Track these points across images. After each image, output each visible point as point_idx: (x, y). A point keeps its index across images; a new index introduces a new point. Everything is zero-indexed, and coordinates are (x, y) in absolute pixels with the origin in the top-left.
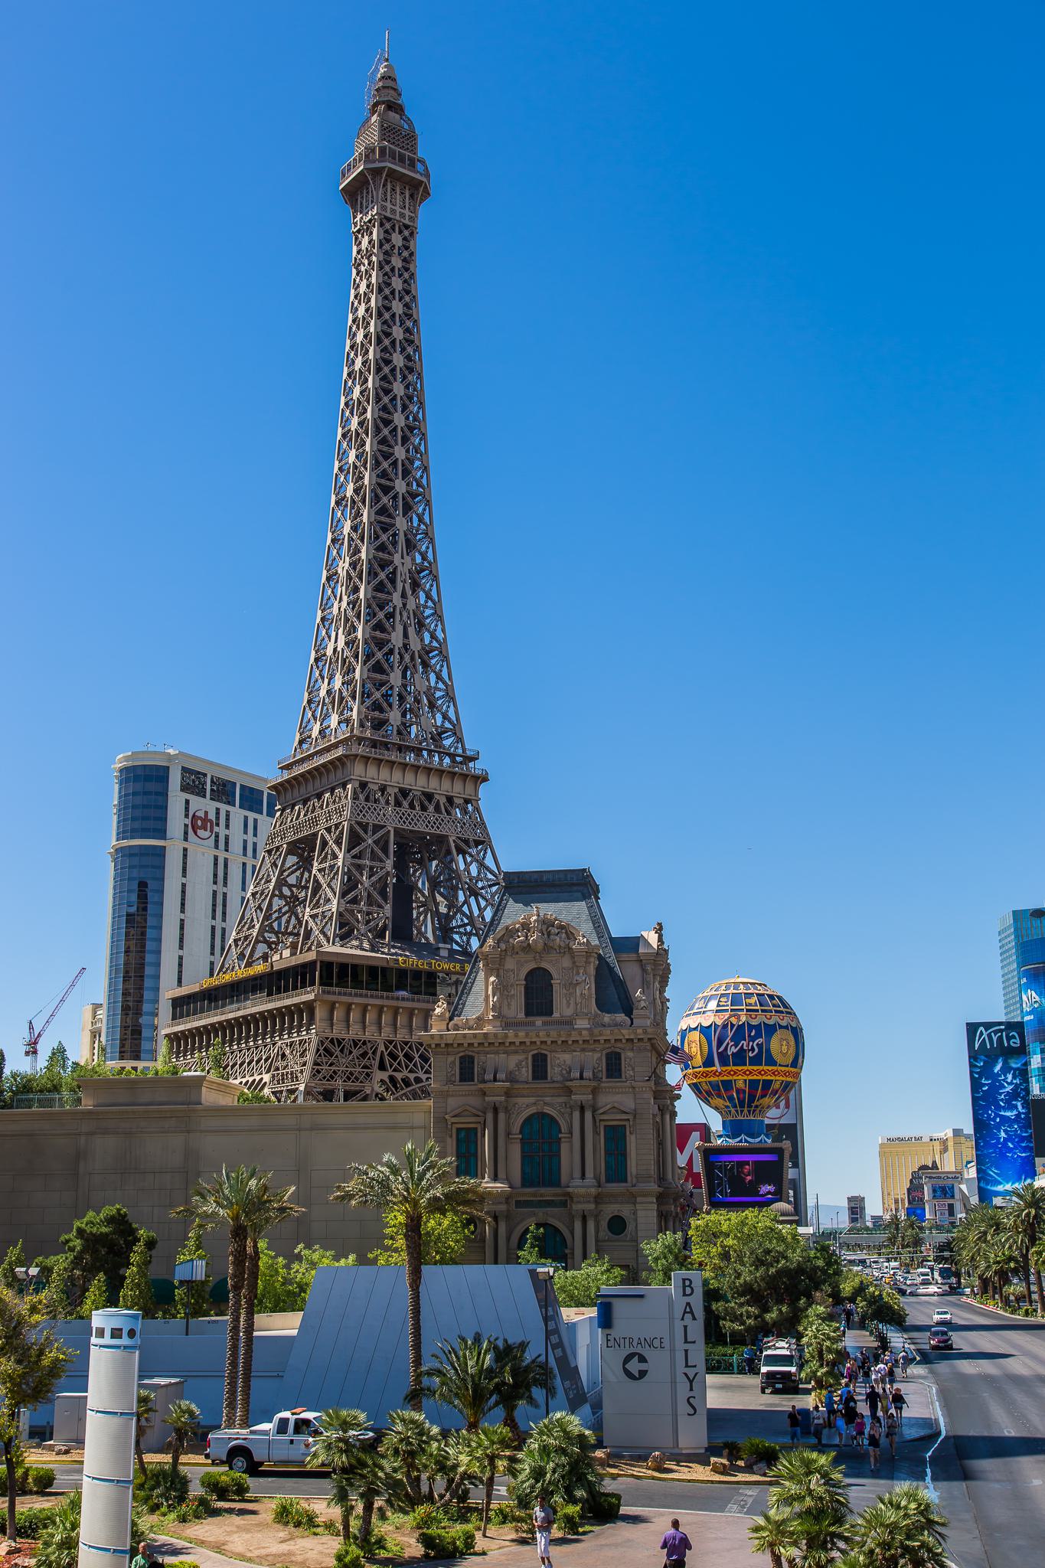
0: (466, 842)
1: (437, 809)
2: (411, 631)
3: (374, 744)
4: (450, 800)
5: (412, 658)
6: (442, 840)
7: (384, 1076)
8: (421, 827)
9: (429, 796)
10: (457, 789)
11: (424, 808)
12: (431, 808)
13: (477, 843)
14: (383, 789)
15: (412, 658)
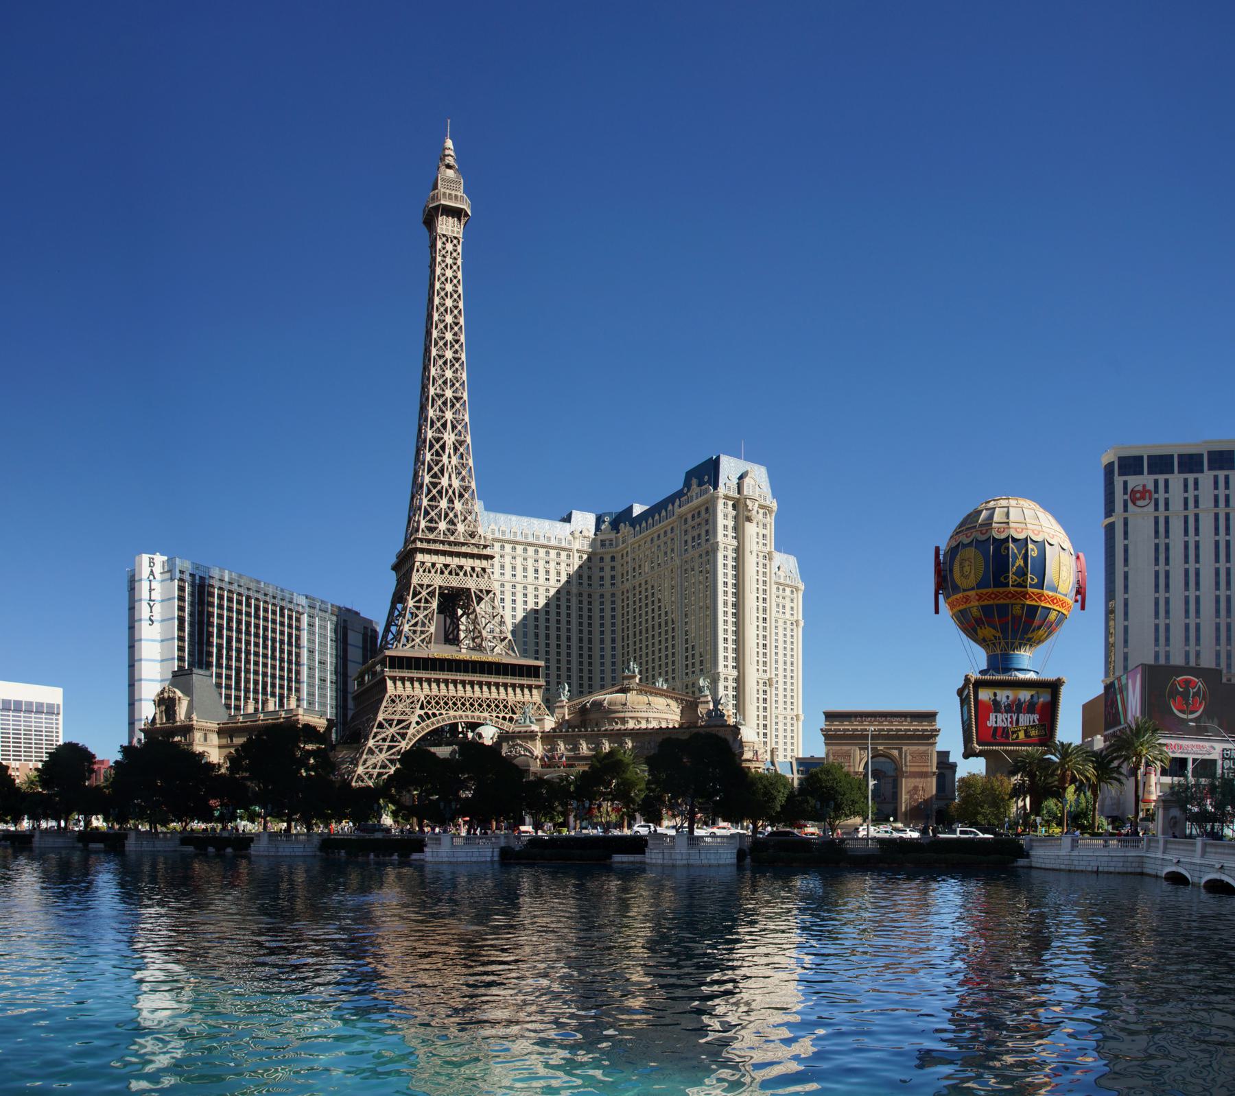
0: (481, 591)
1: (465, 574)
2: (453, 476)
3: (428, 541)
4: (473, 569)
5: (454, 493)
6: (469, 589)
7: (422, 712)
8: (455, 584)
9: (461, 568)
10: (478, 564)
11: (457, 574)
12: (461, 574)
13: (488, 592)
14: (433, 565)
15: (454, 493)
